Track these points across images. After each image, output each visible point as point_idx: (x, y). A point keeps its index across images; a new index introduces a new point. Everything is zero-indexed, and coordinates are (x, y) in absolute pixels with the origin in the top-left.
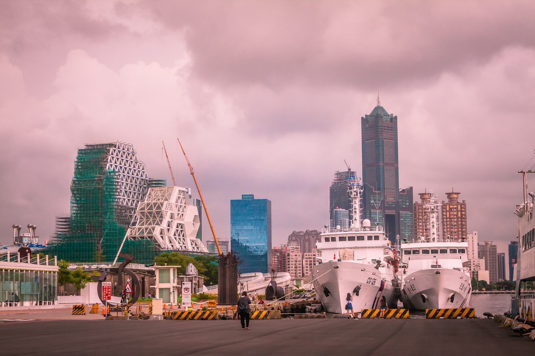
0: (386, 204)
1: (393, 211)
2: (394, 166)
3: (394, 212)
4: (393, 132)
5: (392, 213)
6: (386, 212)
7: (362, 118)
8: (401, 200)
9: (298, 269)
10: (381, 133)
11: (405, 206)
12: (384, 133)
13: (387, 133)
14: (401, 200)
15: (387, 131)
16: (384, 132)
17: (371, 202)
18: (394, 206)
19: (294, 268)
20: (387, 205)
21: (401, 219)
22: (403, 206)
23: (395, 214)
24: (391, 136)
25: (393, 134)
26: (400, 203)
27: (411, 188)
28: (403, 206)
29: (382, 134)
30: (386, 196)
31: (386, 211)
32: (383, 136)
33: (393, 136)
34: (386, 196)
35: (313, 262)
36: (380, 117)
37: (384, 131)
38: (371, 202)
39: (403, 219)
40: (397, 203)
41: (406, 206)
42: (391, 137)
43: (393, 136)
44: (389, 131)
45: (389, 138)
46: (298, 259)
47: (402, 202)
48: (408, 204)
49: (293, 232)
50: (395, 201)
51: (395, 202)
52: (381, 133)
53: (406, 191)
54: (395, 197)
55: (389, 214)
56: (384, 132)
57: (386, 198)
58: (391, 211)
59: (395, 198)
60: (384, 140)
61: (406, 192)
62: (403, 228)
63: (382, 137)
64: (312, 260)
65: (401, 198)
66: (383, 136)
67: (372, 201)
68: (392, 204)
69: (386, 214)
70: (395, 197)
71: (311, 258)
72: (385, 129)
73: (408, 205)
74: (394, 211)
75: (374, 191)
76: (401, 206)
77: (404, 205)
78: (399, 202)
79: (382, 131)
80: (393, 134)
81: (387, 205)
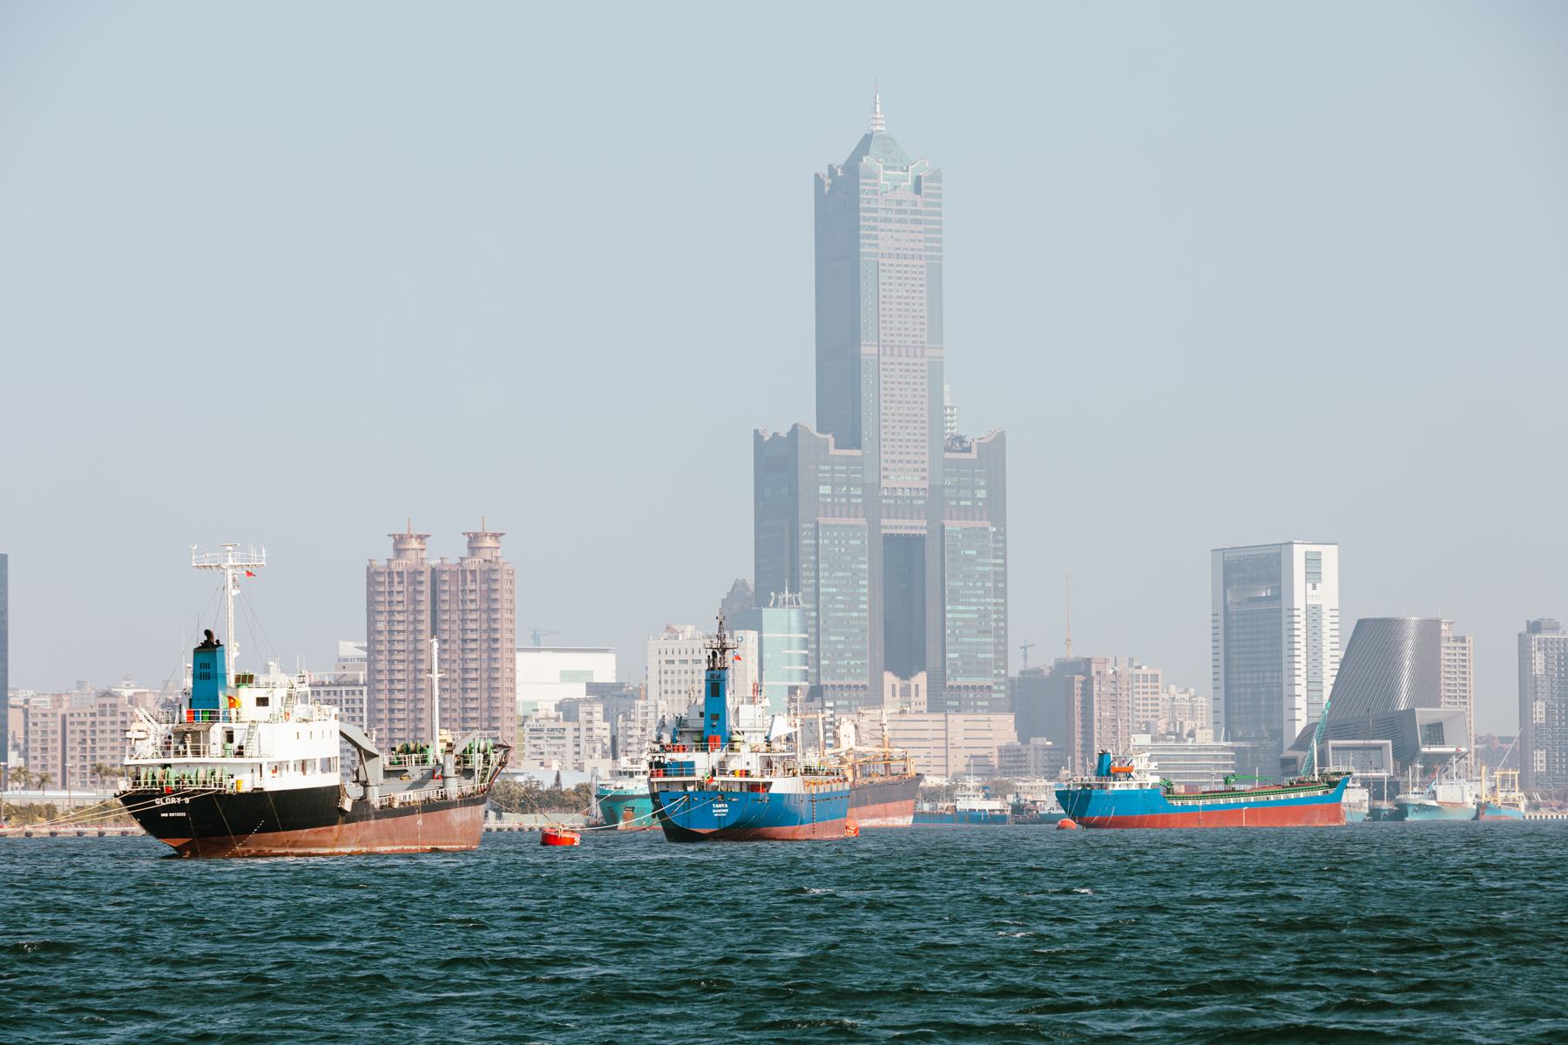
2: (923, 356)
3: (922, 528)
4: (921, 227)
6: (886, 527)
7: (817, 175)
8: (955, 480)
9: (50, 753)
10: (869, 237)
11: (969, 503)
12: (882, 234)
13: (896, 235)
14: (955, 480)
15: (898, 226)
16: (882, 230)
17: (821, 492)
18: (921, 502)
19: (38, 753)
20: (892, 501)
22: (962, 503)
23: (924, 532)
24: (912, 245)
25: (921, 237)
26: (946, 491)
27: (1000, 439)
28: (962, 503)
29: (876, 237)
30: (886, 469)
31: (884, 522)
32: (877, 246)
33: (921, 246)
34: (886, 469)
35: (88, 732)
36: (864, 178)
37: (881, 225)
38: (821, 492)
42: (913, 250)
43: (921, 246)
44: (904, 226)
45: (905, 252)
46: (51, 724)
48: (981, 494)
49: (735, 585)
50: (926, 487)
51: (924, 489)
52: (869, 237)
53: (974, 450)
54: (924, 470)
56: (882, 230)
58: (908, 522)
59: (924, 474)
60: (882, 261)
61: (974, 450)
62: (957, 584)
63: (874, 250)
64: (87, 728)
66: (877, 246)
67: (825, 490)
68: (911, 498)
69: (886, 534)
70: (924, 470)
71: (83, 723)
72: (886, 220)
73: (981, 499)
75: (832, 451)
76: (954, 503)
77: (966, 499)
79: (875, 228)
80: (921, 237)
81: (892, 501)
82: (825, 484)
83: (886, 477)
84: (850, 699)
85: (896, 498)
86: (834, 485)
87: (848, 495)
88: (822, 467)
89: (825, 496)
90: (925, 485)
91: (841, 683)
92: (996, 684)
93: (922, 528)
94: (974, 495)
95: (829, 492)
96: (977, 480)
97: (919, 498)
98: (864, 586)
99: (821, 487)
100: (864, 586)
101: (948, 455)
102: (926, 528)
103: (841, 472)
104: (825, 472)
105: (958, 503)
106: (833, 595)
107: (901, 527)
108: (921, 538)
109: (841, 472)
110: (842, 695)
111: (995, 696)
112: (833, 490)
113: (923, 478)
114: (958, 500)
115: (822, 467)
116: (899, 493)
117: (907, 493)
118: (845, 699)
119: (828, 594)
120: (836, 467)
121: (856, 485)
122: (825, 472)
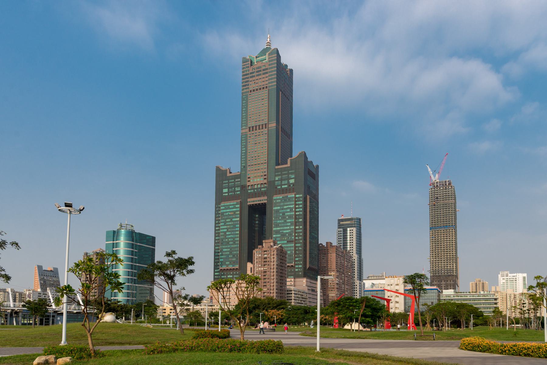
0: (251, 189)
1: (261, 198)
3: (265, 200)
5: (260, 201)
6: (250, 202)
14: (280, 177)
20: (252, 191)
21: (274, 208)
22: (283, 187)
23: (266, 201)
26: (276, 182)
28: (283, 187)
31: (249, 200)
34: (249, 178)
39: (279, 208)
40: (271, 184)
41: (289, 185)
47: (281, 180)
48: (292, 181)
51: (266, 183)
54: (265, 175)
55: (259, 204)
57: (249, 179)
58: (258, 199)
59: (266, 177)
62: (279, 222)
65: (278, 175)
68: (261, 188)
69: (250, 205)
70: (265, 175)
74: (266, 198)
76: (279, 187)
77: (285, 185)
78: (275, 181)
81: (252, 191)
82: (225, 188)
83: (249, 181)
84: (233, 275)
85: (254, 189)
86: (228, 188)
87: (235, 191)
88: (224, 182)
89: (225, 193)
90: (266, 181)
91: (227, 268)
92: (296, 265)
93: (265, 200)
94: (288, 182)
95: (227, 191)
96: (290, 175)
97: (264, 188)
98: (237, 227)
99: (224, 190)
100: (237, 227)
101: (277, 167)
102: (267, 200)
103: (232, 182)
104: (225, 183)
105: (281, 187)
106: (225, 233)
107: (256, 201)
108: (264, 205)
109: (232, 182)
110: (230, 273)
111: (297, 270)
112: (228, 190)
113: (265, 179)
114: (281, 185)
115: (224, 182)
116: (256, 187)
117: (259, 186)
118: (231, 275)
119: (223, 232)
120: (230, 181)
121: (238, 187)
122: (225, 183)
